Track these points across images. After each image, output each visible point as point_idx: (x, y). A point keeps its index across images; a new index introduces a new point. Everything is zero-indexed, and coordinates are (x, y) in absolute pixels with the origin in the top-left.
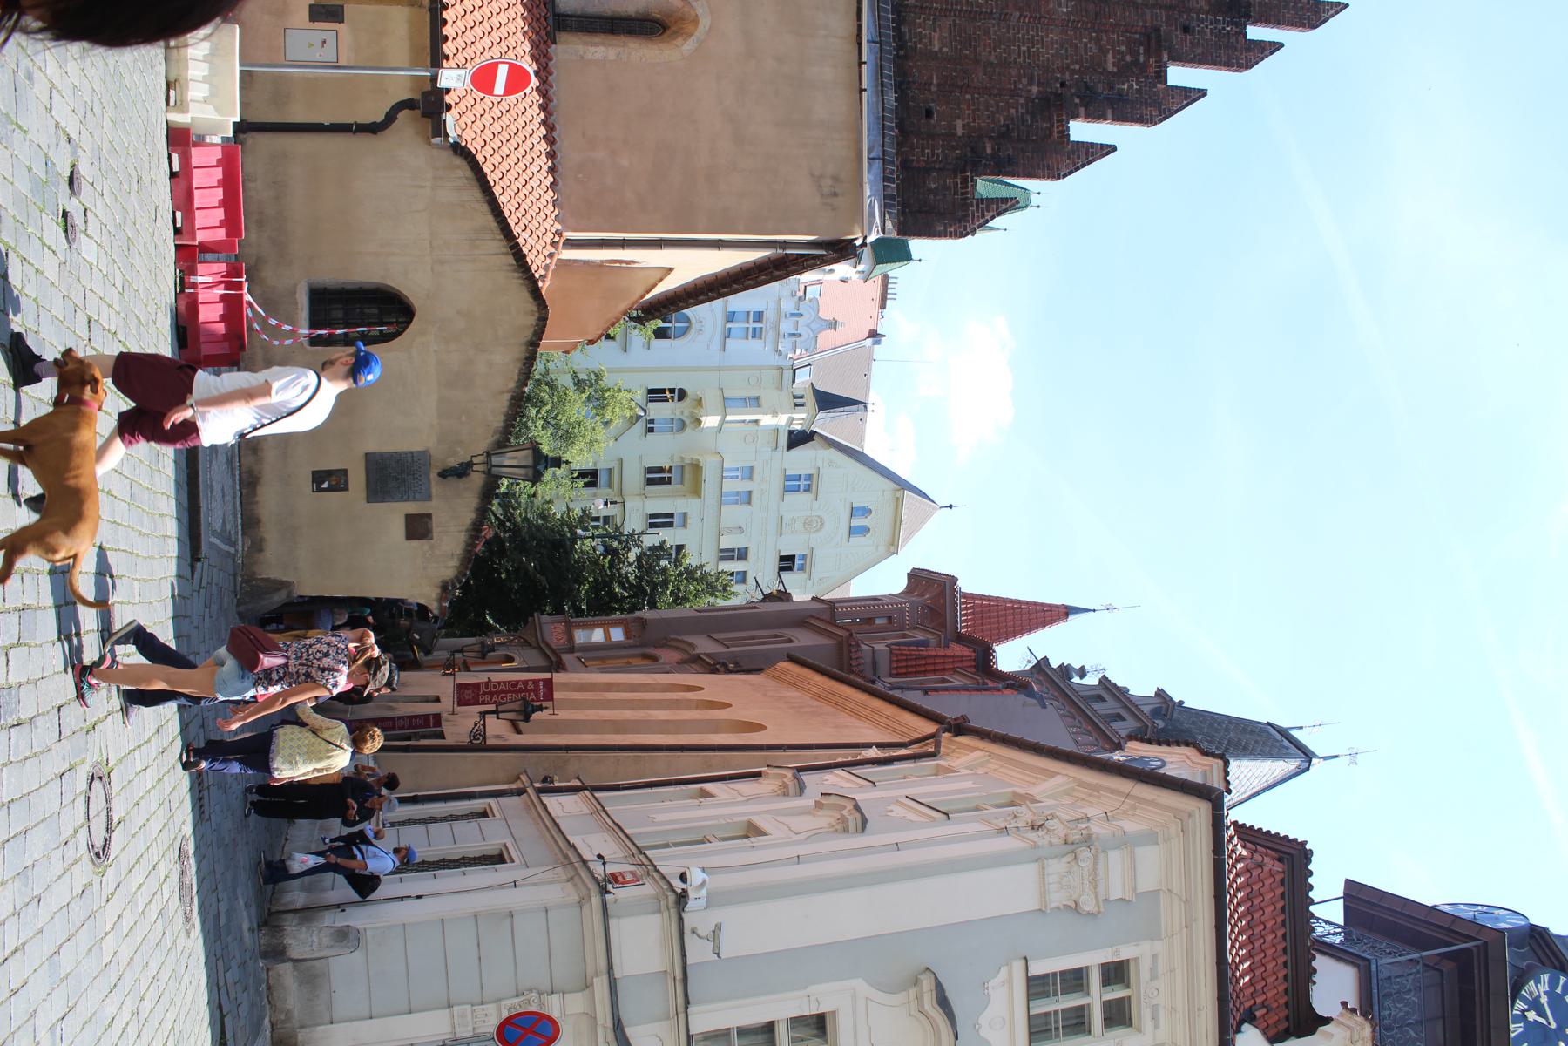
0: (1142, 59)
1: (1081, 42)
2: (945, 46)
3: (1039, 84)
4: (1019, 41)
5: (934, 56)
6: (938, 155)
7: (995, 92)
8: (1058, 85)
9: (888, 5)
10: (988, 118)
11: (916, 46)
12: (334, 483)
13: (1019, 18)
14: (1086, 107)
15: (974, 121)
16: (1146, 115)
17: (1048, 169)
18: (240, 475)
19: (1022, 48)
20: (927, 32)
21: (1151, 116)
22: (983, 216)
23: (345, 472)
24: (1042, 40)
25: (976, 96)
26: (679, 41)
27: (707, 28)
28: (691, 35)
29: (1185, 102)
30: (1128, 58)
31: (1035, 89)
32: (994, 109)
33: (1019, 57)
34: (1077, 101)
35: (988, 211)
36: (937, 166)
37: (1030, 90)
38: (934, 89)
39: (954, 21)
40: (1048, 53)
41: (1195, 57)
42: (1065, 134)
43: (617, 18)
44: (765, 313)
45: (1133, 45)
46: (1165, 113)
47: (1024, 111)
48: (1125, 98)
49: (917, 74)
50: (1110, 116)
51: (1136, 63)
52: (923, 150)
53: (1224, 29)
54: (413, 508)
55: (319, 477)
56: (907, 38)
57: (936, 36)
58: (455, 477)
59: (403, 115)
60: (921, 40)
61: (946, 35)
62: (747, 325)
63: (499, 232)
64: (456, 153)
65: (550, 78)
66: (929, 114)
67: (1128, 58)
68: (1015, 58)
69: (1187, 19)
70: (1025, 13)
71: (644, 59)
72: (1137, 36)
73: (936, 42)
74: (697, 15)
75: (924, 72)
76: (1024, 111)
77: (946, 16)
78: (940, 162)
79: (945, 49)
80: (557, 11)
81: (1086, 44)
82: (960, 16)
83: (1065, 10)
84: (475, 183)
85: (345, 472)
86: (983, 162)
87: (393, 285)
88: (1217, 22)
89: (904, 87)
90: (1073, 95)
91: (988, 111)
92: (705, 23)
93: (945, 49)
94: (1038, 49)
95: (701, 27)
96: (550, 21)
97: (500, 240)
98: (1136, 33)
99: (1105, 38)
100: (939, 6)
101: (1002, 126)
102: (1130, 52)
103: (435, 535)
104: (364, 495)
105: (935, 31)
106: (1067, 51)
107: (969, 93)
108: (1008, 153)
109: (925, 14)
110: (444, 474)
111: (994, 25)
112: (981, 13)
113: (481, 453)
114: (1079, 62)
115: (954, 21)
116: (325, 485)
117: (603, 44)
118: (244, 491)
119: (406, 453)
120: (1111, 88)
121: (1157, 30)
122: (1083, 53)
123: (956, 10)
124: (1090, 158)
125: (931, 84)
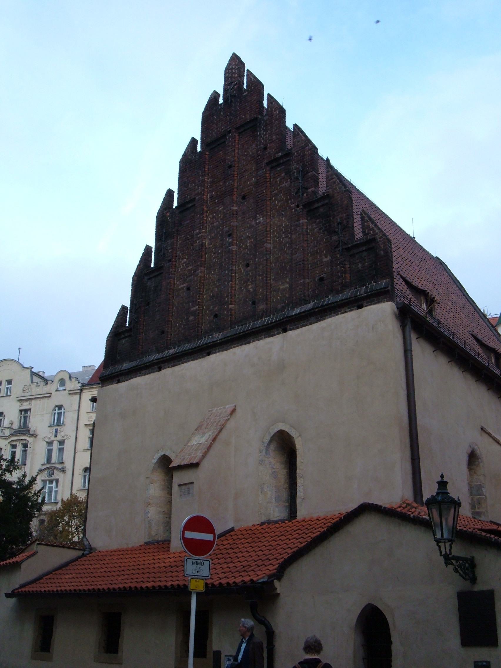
8: (298, 209)
9: (266, 319)
10: (320, 244)
13: (268, 243)
14: (307, 189)
16: (308, 153)
19: (284, 236)
21: (309, 150)
24: (280, 226)
25: (309, 255)
27: (284, 424)
30: (283, 175)
34: (305, 195)
36: (348, 266)
37: (303, 225)
38: (307, 281)
41: (278, 139)
45: (277, 175)
47: (315, 224)
49: (299, 293)
52: (339, 277)
66: (322, 279)
69: (260, 150)
71: (302, 461)
72: (272, 174)
73: (284, 287)
74: (278, 431)
76: (315, 224)
77: (271, 285)
79: (288, 280)
81: (279, 201)
82: (270, 277)
83: (262, 219)
88: (260, 134)
89: (308, 298)
92: (281, 426)
94: (283, 228)
98: (270, 176)
99: (274, 192)
100: (265, 291)
101: (324, 234)
105: (279, 289)
108: (336, 225)
109: (271, 298)
110: (474, 580)
111: (274, 256)
112: (267, 265)
113: (438, 547)
120: (297, 178)
121: (267, 164)
122: (283, 201)
123: (266, 280)
124: (334, 176)
125: (304, 283)
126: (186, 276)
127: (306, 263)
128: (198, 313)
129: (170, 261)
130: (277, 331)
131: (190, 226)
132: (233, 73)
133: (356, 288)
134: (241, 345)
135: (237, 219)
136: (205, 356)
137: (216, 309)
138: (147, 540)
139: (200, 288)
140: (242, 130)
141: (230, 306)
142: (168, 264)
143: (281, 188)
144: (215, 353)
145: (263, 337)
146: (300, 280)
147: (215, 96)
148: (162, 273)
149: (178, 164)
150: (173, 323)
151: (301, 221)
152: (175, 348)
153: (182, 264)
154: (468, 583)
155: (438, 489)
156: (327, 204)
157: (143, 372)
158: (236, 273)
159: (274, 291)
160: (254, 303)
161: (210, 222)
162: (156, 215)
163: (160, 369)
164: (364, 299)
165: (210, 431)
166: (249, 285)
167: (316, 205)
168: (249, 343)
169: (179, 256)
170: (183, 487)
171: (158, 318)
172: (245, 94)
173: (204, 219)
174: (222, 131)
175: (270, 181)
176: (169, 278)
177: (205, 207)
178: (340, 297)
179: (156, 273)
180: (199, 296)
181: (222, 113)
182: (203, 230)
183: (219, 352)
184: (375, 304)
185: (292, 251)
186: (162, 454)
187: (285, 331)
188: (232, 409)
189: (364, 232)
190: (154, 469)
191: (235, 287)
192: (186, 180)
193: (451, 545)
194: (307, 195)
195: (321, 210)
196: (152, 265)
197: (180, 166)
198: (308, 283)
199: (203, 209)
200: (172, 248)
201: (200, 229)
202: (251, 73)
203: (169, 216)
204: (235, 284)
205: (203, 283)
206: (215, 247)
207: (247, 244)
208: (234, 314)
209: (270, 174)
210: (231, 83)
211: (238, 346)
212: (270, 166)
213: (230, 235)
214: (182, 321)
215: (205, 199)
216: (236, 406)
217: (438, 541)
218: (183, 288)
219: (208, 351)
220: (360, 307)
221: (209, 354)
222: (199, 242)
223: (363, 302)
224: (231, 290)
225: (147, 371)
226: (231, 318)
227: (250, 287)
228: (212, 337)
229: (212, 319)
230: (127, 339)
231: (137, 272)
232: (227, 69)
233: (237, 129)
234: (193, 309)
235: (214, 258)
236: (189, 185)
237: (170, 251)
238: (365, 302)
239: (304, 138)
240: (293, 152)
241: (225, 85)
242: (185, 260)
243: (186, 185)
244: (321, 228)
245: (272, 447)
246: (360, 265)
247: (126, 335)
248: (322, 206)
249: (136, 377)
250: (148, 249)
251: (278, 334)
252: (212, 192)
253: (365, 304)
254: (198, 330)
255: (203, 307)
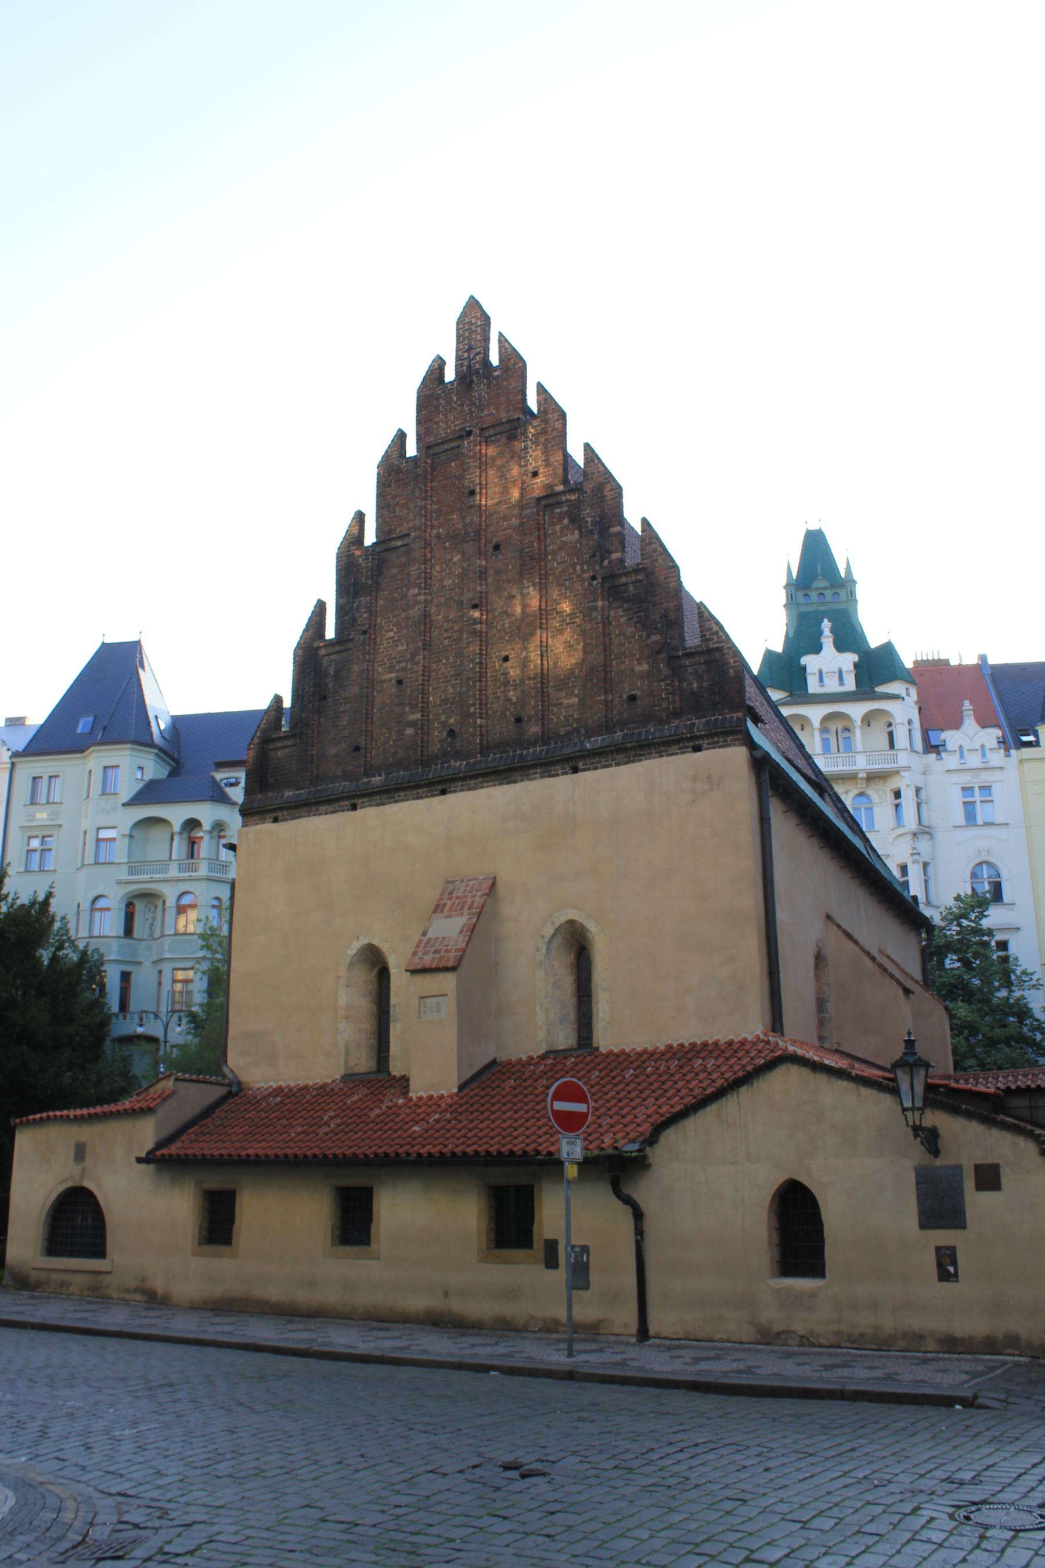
0: (565, 509)
1: (557, 568)
2: (573, 692)
3: (595, 600)
4: (562, 625)
5: (582, 701)
6: (667, 685)
7: (607, 640)
8: (595, 582)
11: (577, 719)
12: (948, 1261)
14: (611, 552)
15: (635, 655)
17: (669, 578)
18: (944, 1353)
20: (563, 710)
21: (611, 490)
22: (717, 633)
23: (938, 1249)
25: (613, 657)
26: (589, 935)
27: (575, 911)
28: (582, 926)
29: (596, 461)
31: (600, 603)
32: (622, 638)
33: (576, 622)
34: (606, 562)
35: (711, 629)
36: (677, 683)
38: (610, 697)
39: (552, 687)
40: (570, 597)
42: (636, 570)
43: (579, 993)
44: (963, 786)
45: (555, 520)
46: (606, 478)
47: (621, 610)
48: (598, 519)
50: (617, 529)
51: (567, 512)
52: (663, 699)
53: (531, 440)
54: (969, 1184)
55: (944, 1276)
56: (570, 728)
57: (566, 702)
58: (939, 1140)
59: (627, 1190)
60: (571, 716)
61: (564, 694)
62: (978, 804)
63: (719, 1101)
64: (656, 1142)
65: (627, 1050)
66: (632, 698)
67: (566, 521)
68: (578, 626)
69: (527, 475)
70: (538, 624)
72: (547, 518)
74: (567, 922)
75: (596, 709)
76: (621, 610)
78: (672, 681)
79: (576, 692)
80: (575, 1046)
81: (558, 563)
84: (680, 1125)
85: (938, 1249)
86: (669, 641)
87: (769, 1199)
90: (601, 567)
91: (624, 644)
92: (572, 914)
93: (576, 692)
95: (575, 917)
96: (580, 1052)
97: (727, 1100)
99: (551, 547)
100: (540, 704)
101: (636, 627)
102: (561, 520)
103: (995, 1161)
104: (959, 1232)
106: (565, 580)
107: (611, 664)
110: (936, 1152)
114: (574, 566)
115: (552, 687)
116: (951, 1269)
117: (597, 1003)
118: (960, 1350)
119: (918, 1189)
120: (591, 532)
123: (542, 688)
124: (654, 540)
125: (606, 701)
126: (394, 661)
127: (609, 669)
128: (422, 724)
129: (365, 632)
130: (562, 769)
131: (399, 578)
132: (471, 332)
133: (690, 719)
134: (500, 784)
135: (486, 580)
136: (437, 795)
137: (452, 721)
138: (342, 1072)
139: (423, 685)
140: (491, 432)
141: (479, 721)
142: (362, 637)
143: (561, 541)
144: (455, 791)
145: (538, 775)
146: (600, 696)
147: (439, 365)
148: (351, 649)
149: (376, 471)
150: (374, 735)
151: (600, 603)
152: (380, 775)
153: (387, 639)
154: (932, 1156)
155: (905, 1048)
156: (641, 581)
157: (323, 808)
158: (486, 668)
159: (553, 705)
160: (519, 720)
161: (436, 577)
162: (336, 551)
163: (354, 807)
164: (702, 737)
165: (462, 915)
166: (509, 690)
167: (624, 580)
168: (515, 782)
169: (381, 623)
170: (429, 1000)
171: (345, 723)
172: (496, 373)
173: (426, 572)
174: (457, 428)
175: (544, 528)
176: (364, 661)
177: (427, 551)
178: (668, 730)
179: (337, 648)
180: (422, 698)
181: (455, 398)
182: (425, 589)
183: (461, 791)
184: (720, 747)
185: (584, 647)
186: (366, 941)
187: (575, 770)
188: (490, 882)
189: (702, 636)
190: (352, 965)
191: (486, 690)
192: (391, 501)
193: (921, 1115)
194: (609, 563)
195: (631, 588)
196: (330, 633)
197: (378, 474)
198: (612, 701)
199: (425, 555)
200: (370, 613)
201: (420, 588)
202: (506, 340)
203: (361, 556)
204: (486, 685)
205: (429, 676)
206: (446, 619)
207: (503, 625)
208: (485, 733)
209: (544, 515)
210: (470, 349)
211: (495, 785)
212: (543, 503)
213: (475, 607)
214: (390, 733)
215: (428, 538)
216: (495, 878)
217: (904, 1110)
218: (390, 680)
219: (440, 787)
220: (697, 749)
221: (443, 792)
222: (418, 610)
223: (701, 742)
224: (480, 694)
225: (330, 808)
226: (481, 740)
227: (511, 693)
228: (449, 767)
229: (445, 736)
230: (287, 750)
231: (302, 642)
232: (459, 322)
233: (483, 430)
234: (412, 717)
235: (446, 638)
236: (397, 510)
237: (365, 615)
238: (706, 742)
239: (602, 469)
240: (585, 489)
241: (458, 350)
242: (391, 634)
243: (391, 507)
244: (632, 618)
245: (556, 943)
246: (695, 685)
247: (285, 743)
248: (632, 583)
249: (309, 816)
250: (321, 607)
251: (563, 774)
252: (439, 527)
253: (705, 746)
254: (422, 751)
255: (428, 716)
